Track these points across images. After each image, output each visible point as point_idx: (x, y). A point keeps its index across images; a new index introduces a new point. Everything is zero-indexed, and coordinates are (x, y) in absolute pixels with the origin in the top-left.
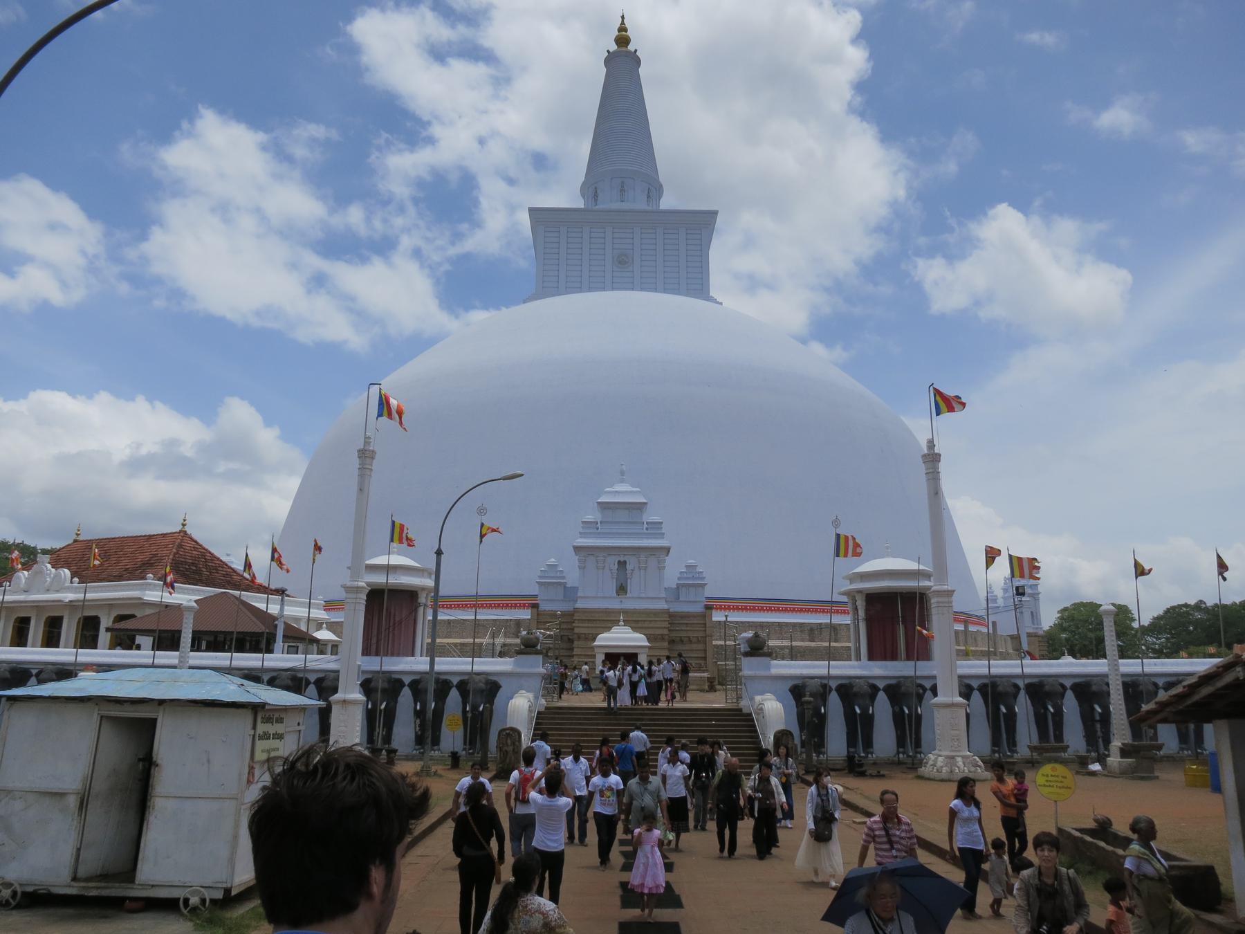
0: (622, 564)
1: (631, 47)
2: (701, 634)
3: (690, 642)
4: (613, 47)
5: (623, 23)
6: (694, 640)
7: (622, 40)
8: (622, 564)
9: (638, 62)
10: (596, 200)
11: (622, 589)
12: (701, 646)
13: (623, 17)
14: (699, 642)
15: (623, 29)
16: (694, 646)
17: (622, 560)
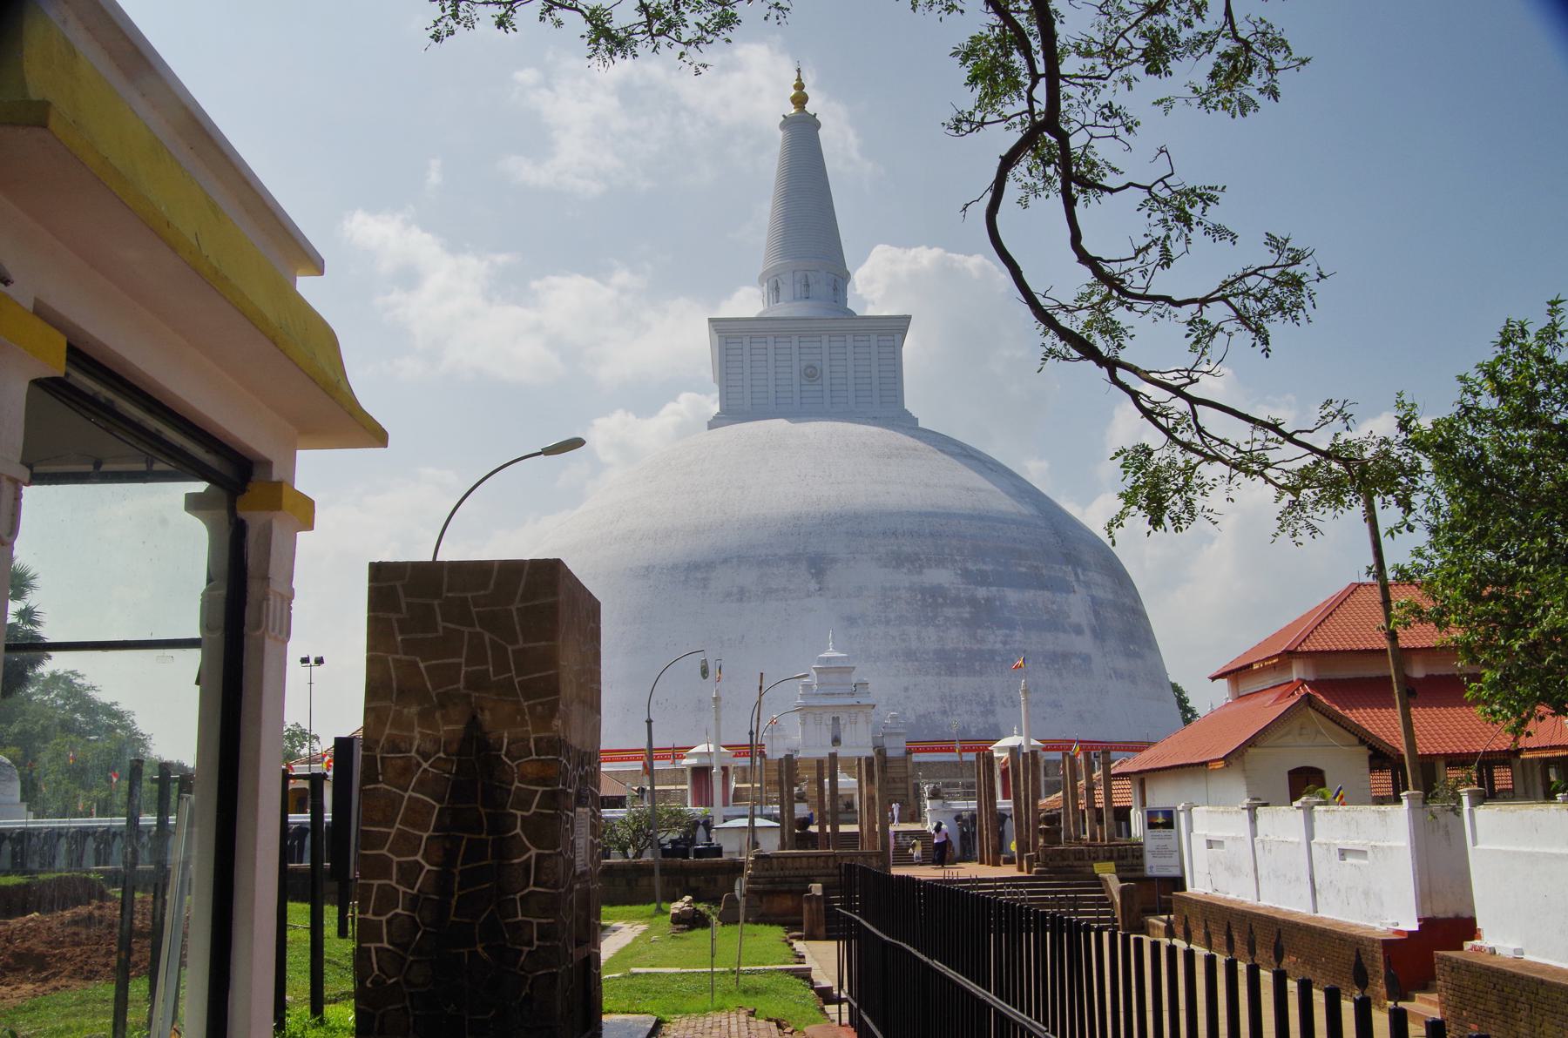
0: (836, 720)
1: (809, 108)
2: (904, 775)
3: (894, 782)
4: (792, 110)
5: (799, 79)
6: (897, 780)
7: (800, 100)
8: (836, 720)
9: (818, 125)
10: (778, 296)
11: (836, 741)
12: (903, 785)
13: (799, 71)
14: (902, 782)
15: (800, 86)
16: (899, 785)
17: (835, 716)
